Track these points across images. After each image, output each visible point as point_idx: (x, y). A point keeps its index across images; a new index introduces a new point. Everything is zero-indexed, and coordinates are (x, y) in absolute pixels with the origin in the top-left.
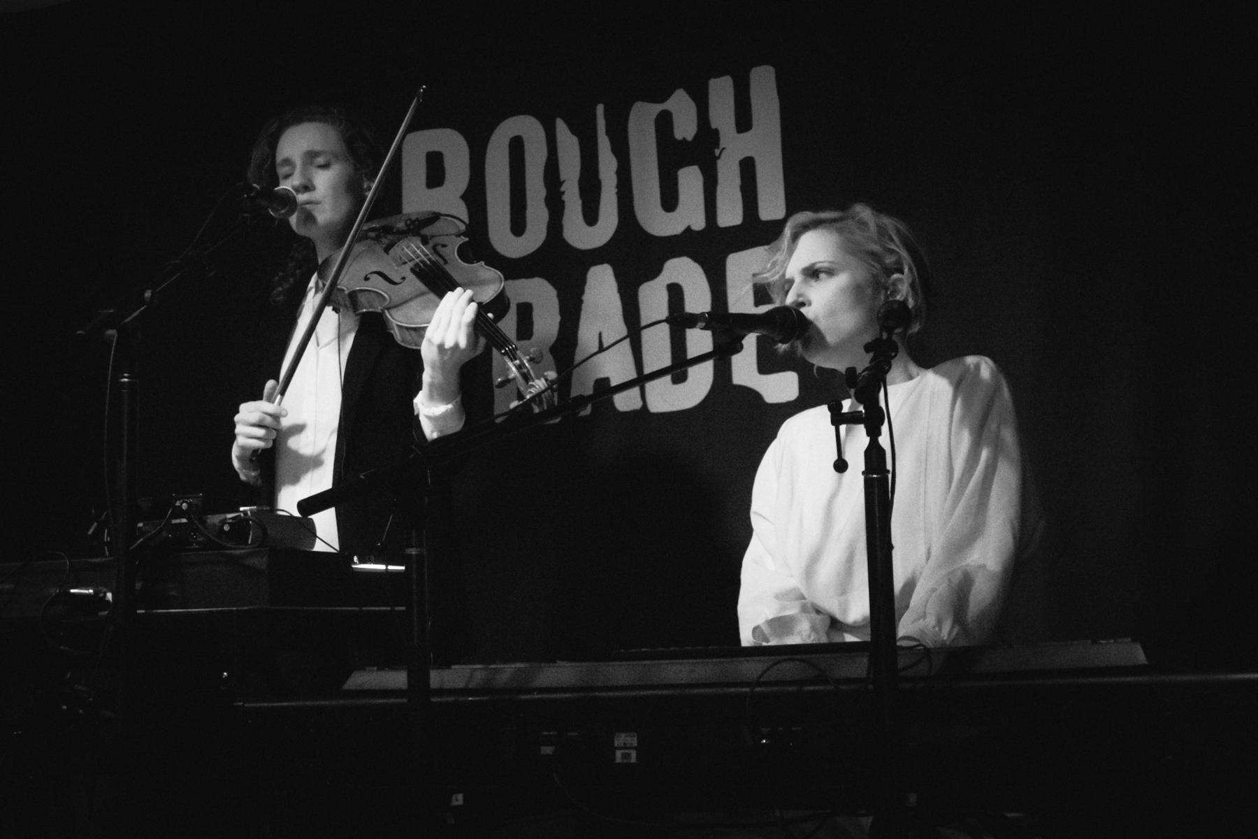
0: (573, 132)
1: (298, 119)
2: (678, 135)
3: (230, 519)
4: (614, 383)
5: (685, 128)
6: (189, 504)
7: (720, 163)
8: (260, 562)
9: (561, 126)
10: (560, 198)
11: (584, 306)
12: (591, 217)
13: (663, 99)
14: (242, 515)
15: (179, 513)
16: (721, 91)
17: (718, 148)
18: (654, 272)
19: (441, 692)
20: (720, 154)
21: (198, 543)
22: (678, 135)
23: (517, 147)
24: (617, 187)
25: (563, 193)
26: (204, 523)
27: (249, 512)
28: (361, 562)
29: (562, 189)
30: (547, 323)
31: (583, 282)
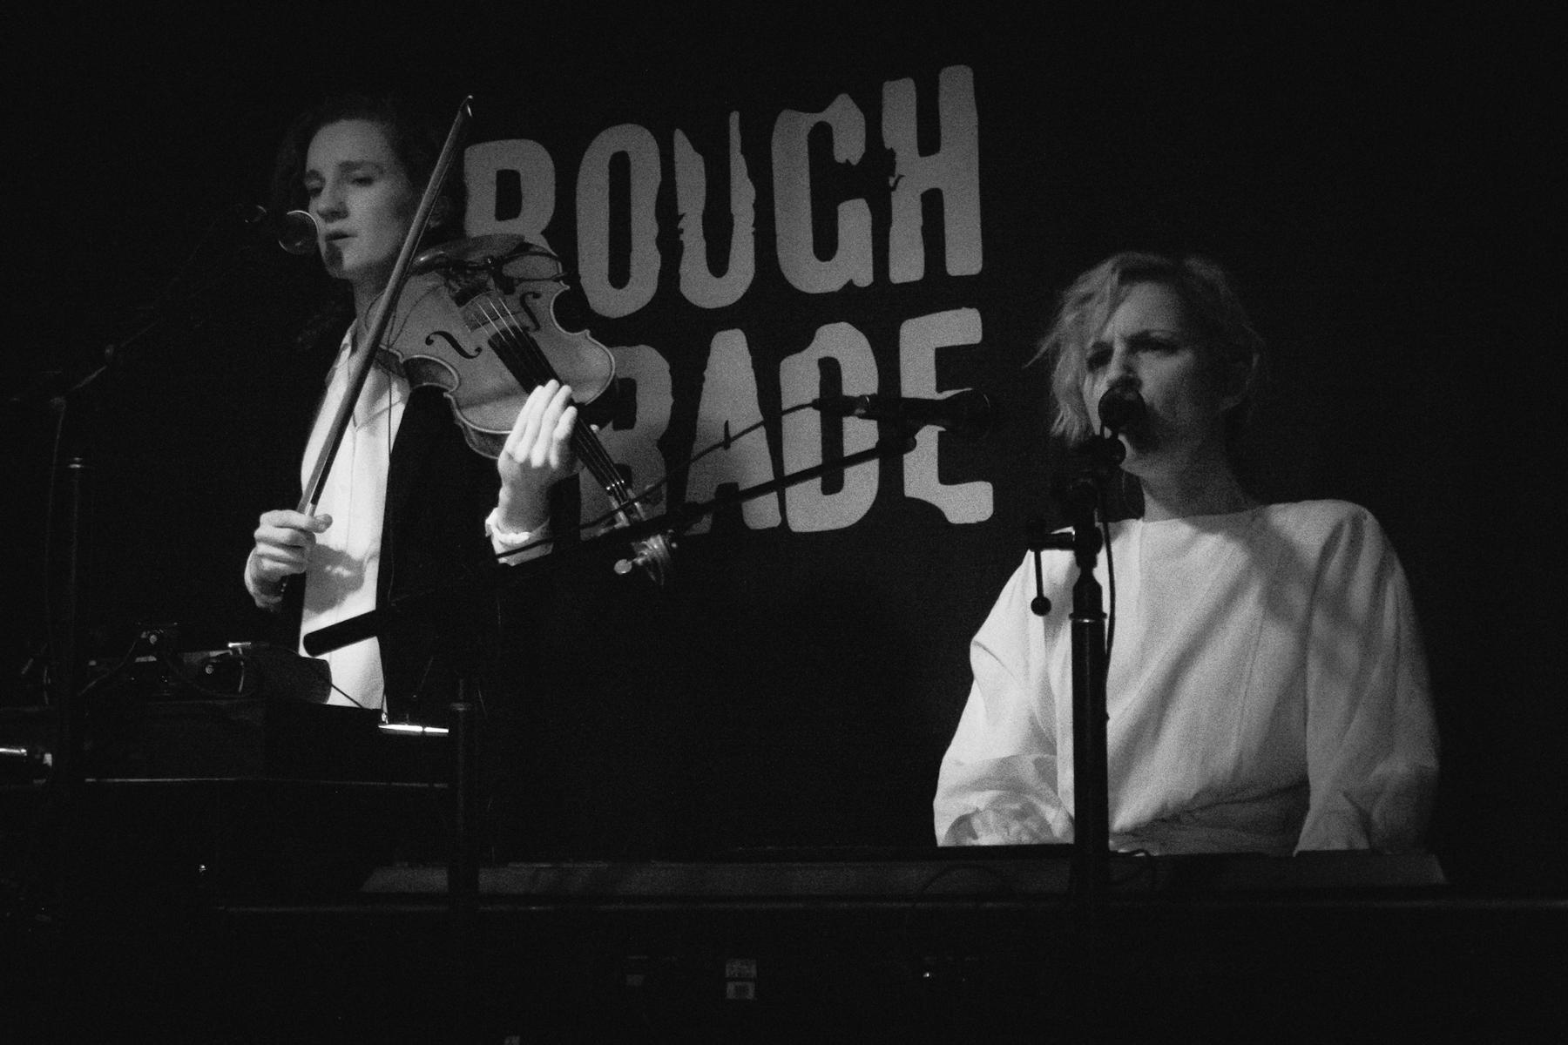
2: (841, 155)
3: (213, 658)
5: (849, 147)
6: (160, 637)
7: (893, 194)
9: (680, 139)
12: (718, 263)
13: (820, 108)
14: (231, 653)
15: (147, 649)
16: (900, 99)
17: (894, 176)
18: (802, 341)
20: (896, 182)
22: (841, 155)
23: (620, 167)
24: (754, 225)
25: (681, 231)
28: (391, 722)
29: (681, 225)
30: (655, 405)
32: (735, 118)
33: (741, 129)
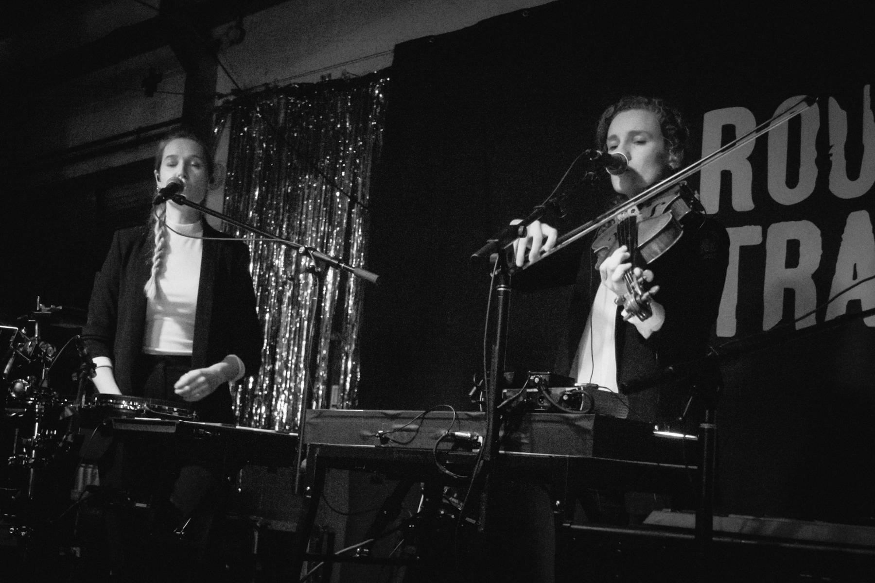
0: (843, 107)
1: (626, 107)
3: (568, 391)
4: (865, 307)
6: (540, 379)
8: (588, 424)
9: (833, 103)
10: (829, 158)
11: (842, 243)
14: (577, 389)
15: (532, 385)
19: (721, 533)
21: (544, 407)
25: (831, 155)
26: (549, 393)
27: (582, 388)
28: (660, 429)
29: (830, 153)
31: (844, 224)
32: (867, 89)
33: (871, 95)
